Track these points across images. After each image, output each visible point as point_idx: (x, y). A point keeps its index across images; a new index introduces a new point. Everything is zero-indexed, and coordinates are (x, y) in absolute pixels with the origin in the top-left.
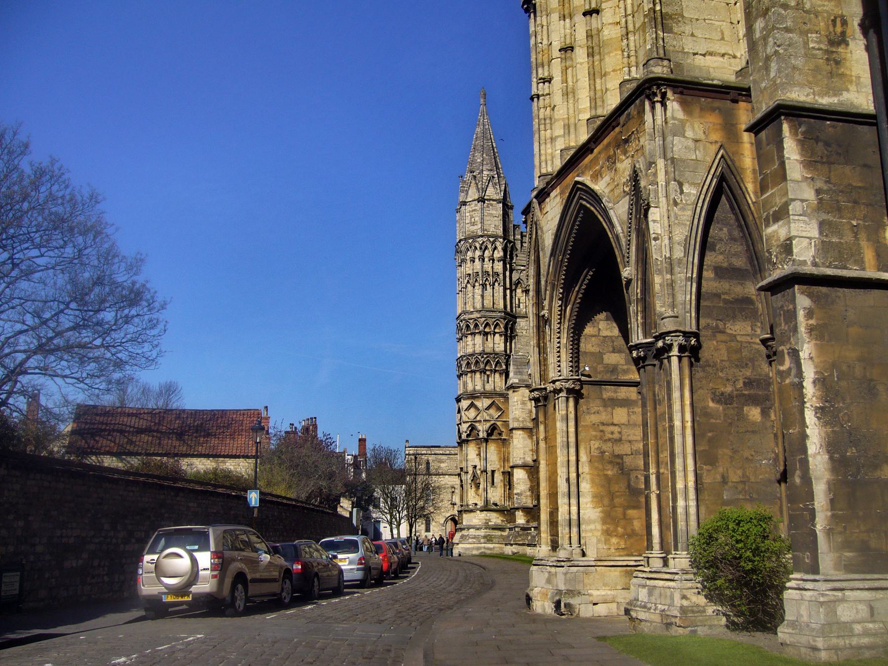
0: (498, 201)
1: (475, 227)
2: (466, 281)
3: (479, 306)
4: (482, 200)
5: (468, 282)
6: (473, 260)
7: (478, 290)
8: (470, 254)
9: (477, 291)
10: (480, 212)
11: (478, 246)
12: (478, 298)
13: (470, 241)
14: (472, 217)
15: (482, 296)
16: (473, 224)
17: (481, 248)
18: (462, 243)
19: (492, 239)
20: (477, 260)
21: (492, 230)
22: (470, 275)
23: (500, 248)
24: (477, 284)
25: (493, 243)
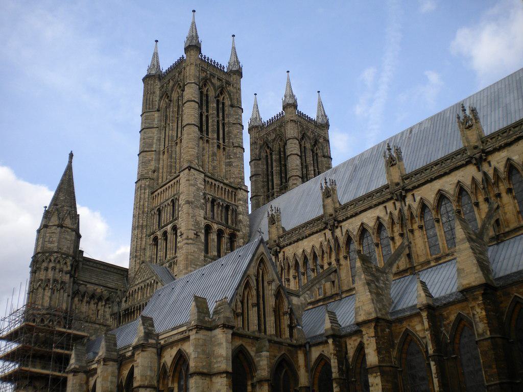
0: (73, 230)
1: (52, 245)
2: (38, 284)
3: (46, 304)
4: (61, 226)
5: (40, 285)
6: (46, 269)
7: (48, 293)
8: (45, 265)
9: (46, 293)
10: (58, 235)
11: (52, 259)
12: (47, 299)
13: (47, 254)
14: (51, 237)
15: (51, 298)
16: (51, 242)
17: (55, 261)
18: (39, 255)
19: (64, 256)
20: (50, 270)
21: (65, 250)
22: (42, 280)
23: (69, 264)
24: (47, 288)
25: (64, 259)
